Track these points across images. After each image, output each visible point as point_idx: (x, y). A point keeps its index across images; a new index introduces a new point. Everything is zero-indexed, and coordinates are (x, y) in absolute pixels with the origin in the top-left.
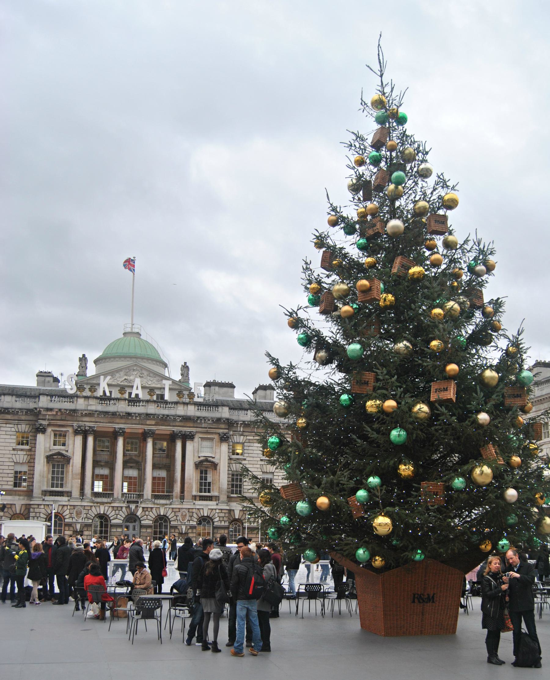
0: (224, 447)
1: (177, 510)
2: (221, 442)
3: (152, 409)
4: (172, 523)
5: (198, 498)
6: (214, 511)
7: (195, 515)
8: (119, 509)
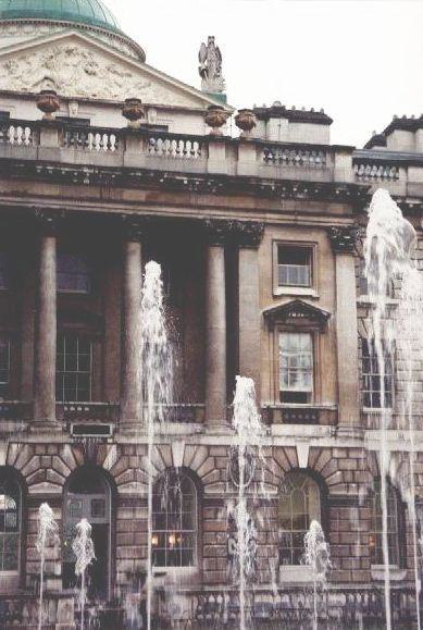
2: (334, 256)
3: (136, 157)
5: (277, 416)
6: (326, 455)
8: (52, 450)
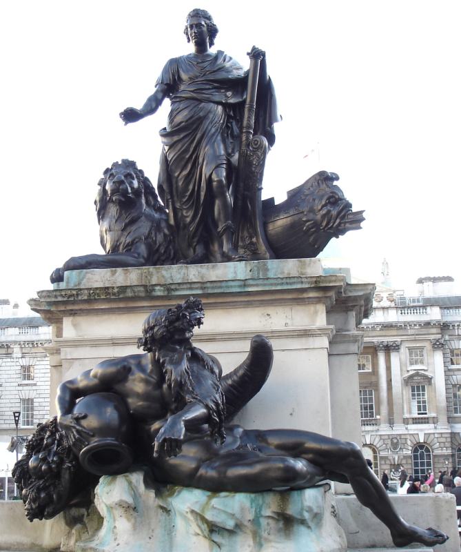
0: (438, 358)
1: (386, 437)
4: (381, 453)
5: (411, 421)
6: (432, 436)
7: (409, 442)
